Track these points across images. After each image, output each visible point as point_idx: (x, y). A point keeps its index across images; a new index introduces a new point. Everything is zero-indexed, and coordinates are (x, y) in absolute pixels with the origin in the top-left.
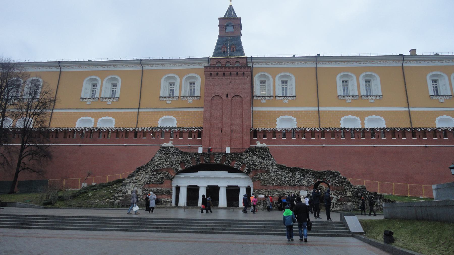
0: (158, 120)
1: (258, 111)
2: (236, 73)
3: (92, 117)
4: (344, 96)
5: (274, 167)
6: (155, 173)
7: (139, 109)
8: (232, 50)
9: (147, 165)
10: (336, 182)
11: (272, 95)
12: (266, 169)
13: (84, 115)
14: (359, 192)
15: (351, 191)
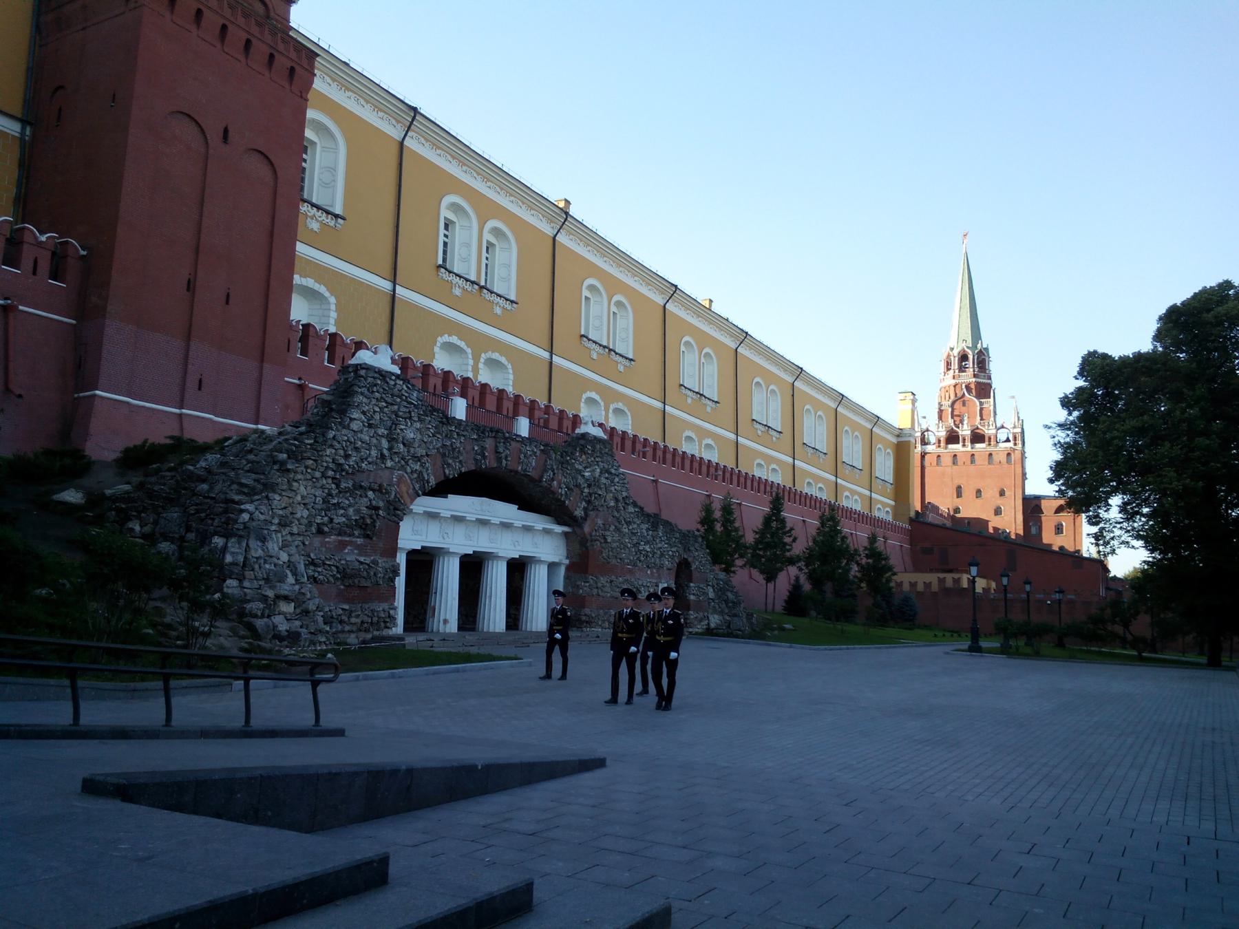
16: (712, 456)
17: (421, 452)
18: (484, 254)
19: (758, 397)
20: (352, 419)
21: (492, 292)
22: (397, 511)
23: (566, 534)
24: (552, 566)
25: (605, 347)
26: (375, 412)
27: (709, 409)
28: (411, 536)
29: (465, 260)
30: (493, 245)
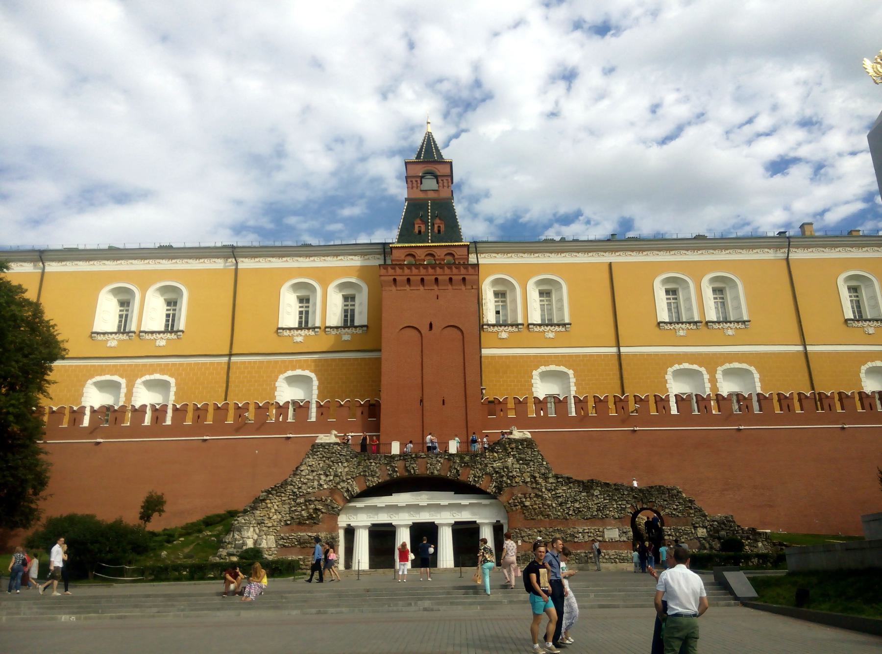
0: (276, 381)
1: (493, 357)
2: (447, 278)
3: (121, 376)
4: (670, 323)
5: (551, 480)
6: (302, 500)
7: (230, 355)
8: (436, 229)
9: (285, 483)
10: (674, 509)
11: (520, 321)
12: (534, 485)
13: (102, 371)
14: (723, 529)
15: (706, 527)
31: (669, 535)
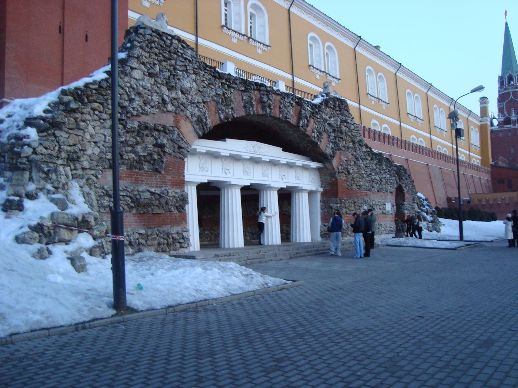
12: (354, 153)
16: (389, 133)
17: (198, 98)
18: (249, 20)
19: (409, 101)
20: (132, 69)
21: (255, 41)
22: (182, 151)
23: (319, 169)
24: (311, 193)
25: (323, 72)
26: (154, 64)
27: (384, 108)
28: (197, 171)
29: (238, 23)
30: (254, 15)
31: (407, 209)
